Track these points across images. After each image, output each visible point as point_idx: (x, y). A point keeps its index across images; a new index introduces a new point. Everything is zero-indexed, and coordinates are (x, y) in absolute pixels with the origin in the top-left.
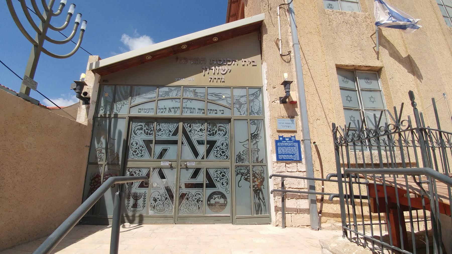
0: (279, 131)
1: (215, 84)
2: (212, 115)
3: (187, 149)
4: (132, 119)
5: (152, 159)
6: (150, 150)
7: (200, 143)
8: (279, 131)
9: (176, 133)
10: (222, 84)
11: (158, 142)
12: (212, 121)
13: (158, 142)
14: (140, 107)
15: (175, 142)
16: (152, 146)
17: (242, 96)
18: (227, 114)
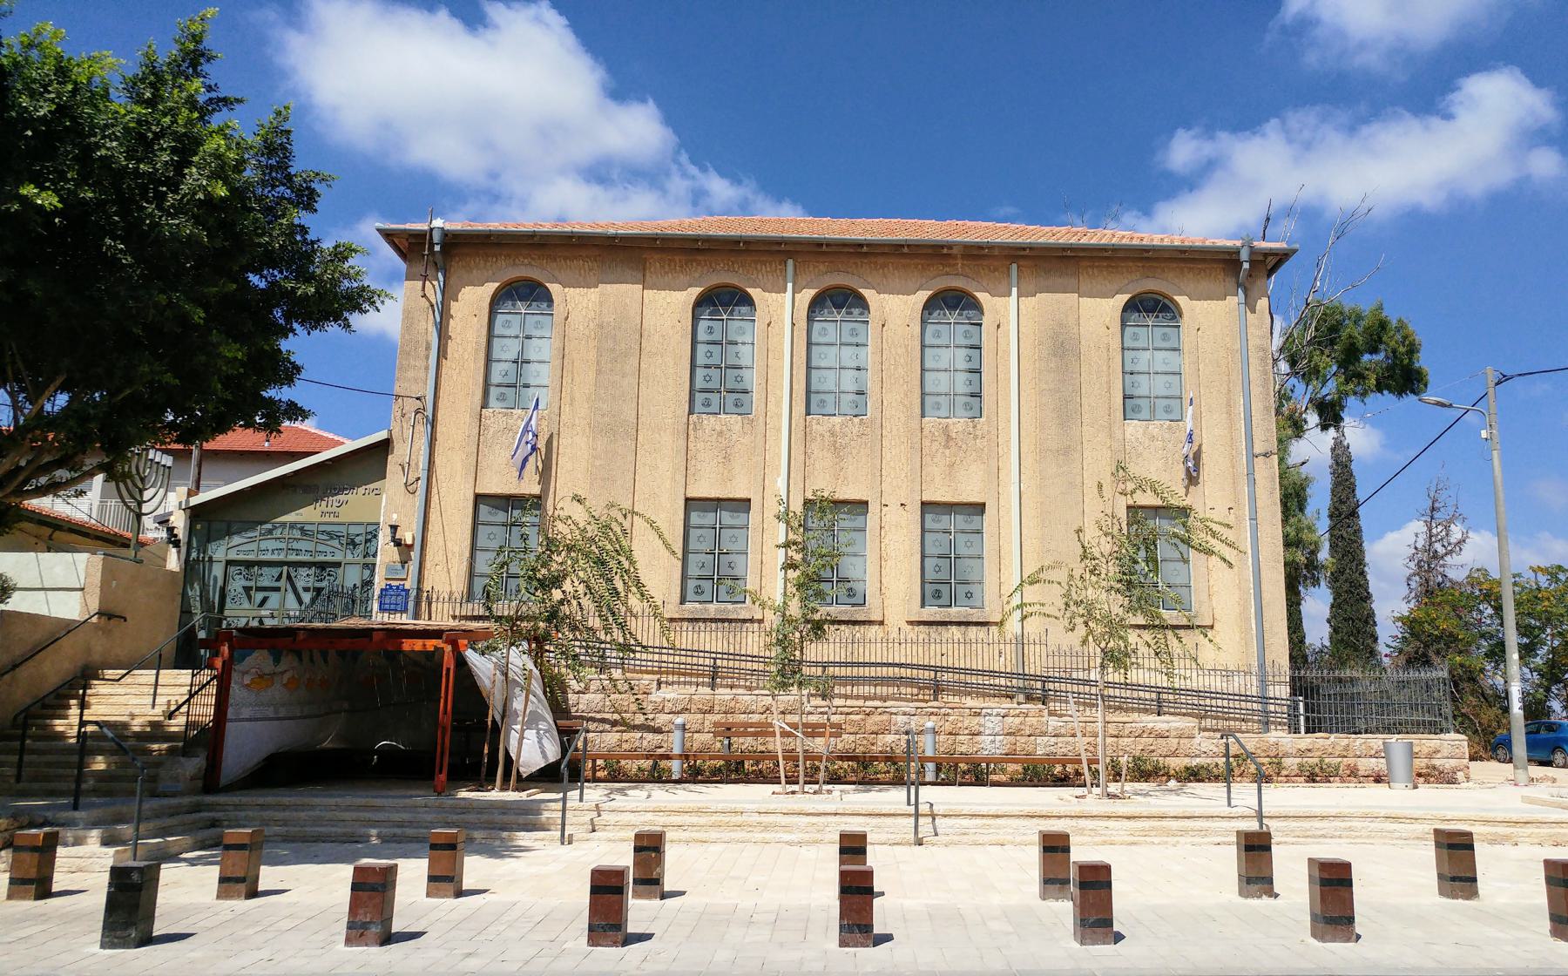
0: (387, 579)
1: (327, 519)
2: (321, 558)
3: (291, 597)
4: (229, 563)
5: (251, 607)
6: (249, 598)
7: (306, 589)
8: (387, 579)
9: (279, 578)
10: (336, 520)
11: (259, 589)
12: (322, 566)
13: (259, 589)
14: (240, 548)
15: (277, 589)
16: (252, 593)
18: (337, 558)
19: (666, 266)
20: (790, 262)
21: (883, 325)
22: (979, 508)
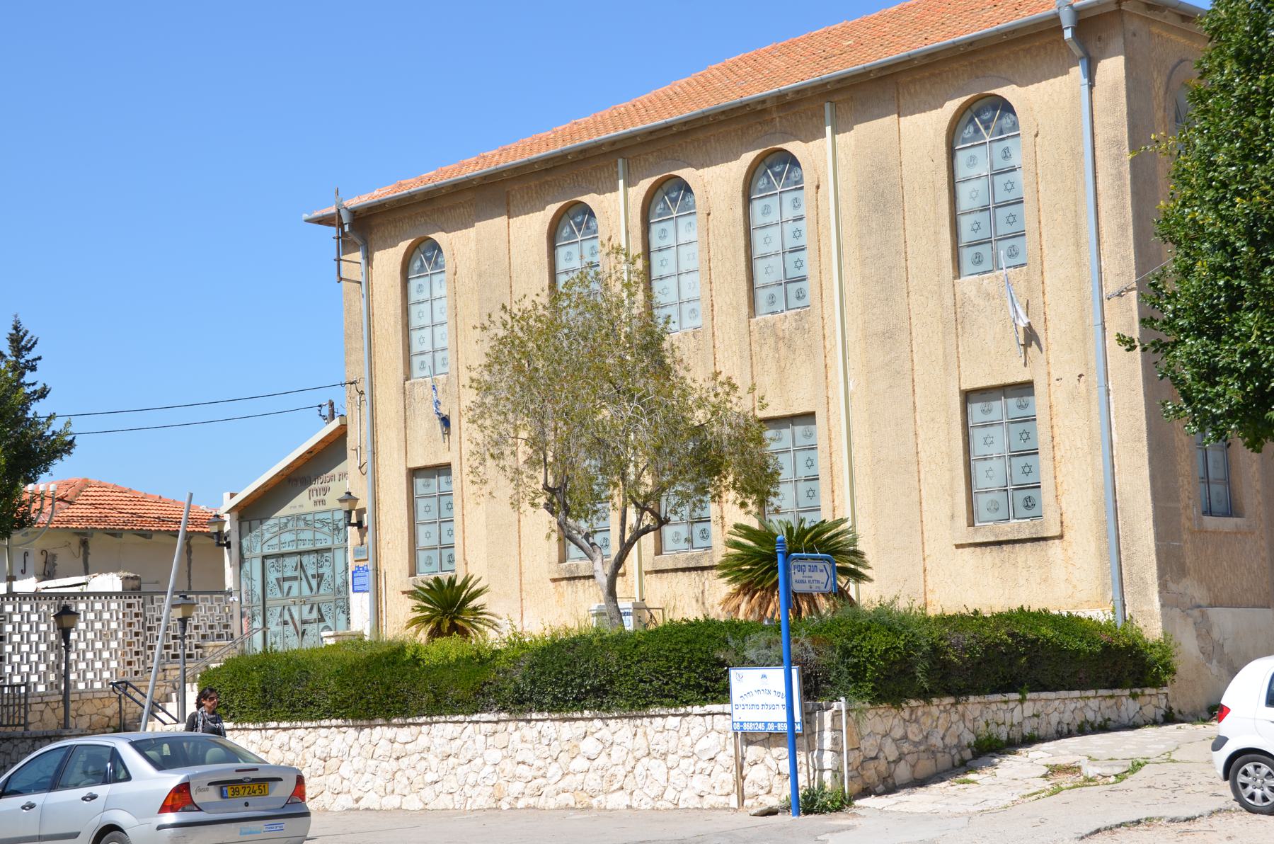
0: (356, 561)
4: (265, 557)
7: (313, 576)
8: (356, 561)
17: (340, 520)
19: (526, 196)
20: (620, 161)
21: (709, 214)
22: (809, 417)
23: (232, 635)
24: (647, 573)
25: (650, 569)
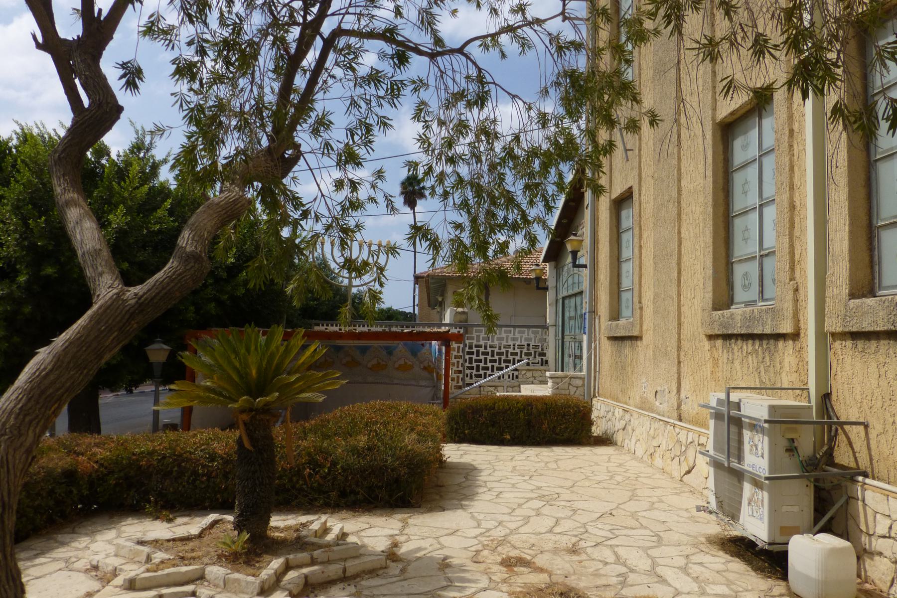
4: (564, 298)
23: (547, 362)
24: (834, 335)
25: (839, 329)
